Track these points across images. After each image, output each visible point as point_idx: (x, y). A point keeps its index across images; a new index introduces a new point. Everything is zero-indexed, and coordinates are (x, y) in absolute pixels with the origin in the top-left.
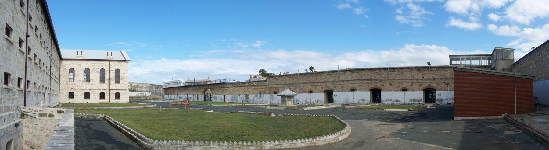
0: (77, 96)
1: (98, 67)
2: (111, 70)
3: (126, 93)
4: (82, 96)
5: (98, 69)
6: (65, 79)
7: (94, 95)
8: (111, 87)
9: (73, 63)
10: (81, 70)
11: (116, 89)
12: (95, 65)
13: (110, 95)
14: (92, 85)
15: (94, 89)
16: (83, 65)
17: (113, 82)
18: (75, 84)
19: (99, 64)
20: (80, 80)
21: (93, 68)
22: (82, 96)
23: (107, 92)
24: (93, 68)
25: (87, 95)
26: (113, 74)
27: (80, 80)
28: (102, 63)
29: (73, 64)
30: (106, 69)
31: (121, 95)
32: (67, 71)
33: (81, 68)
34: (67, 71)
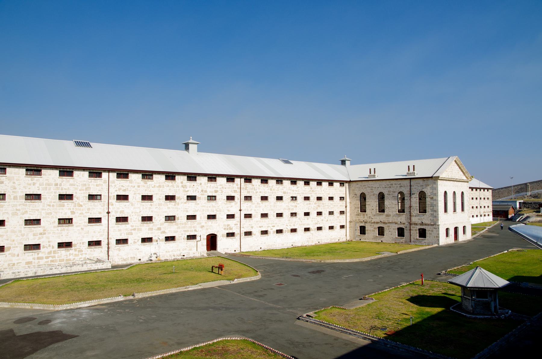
0: (369, 232)
1: (395, 190)
2: (413, 194)
3: (434, 229)
4: (374, 231)
5: (394, 192)
6: (356, 208)
7: (390, 231)
8: (414, 219)
9: (364, 186)
10: (374, 195)
11: (420, 222)
12: (390, 187)
13: (412, 231)
14: (387, 216)
15: (390, 222)
16: (376, 188)
17: (415, 211)
18: (367, 215)
19: (396, 186)
20: (373, 209)
21: (389, 191)
22: (374, 231)
23: (406, 227)
24: (389, 191)
25: (381, 231)
26: (415, 200)
27: (373, 209)
28: (400, 184)
29: (364, 187)
30: (406, 191)
31: (427, 232)
32: (357, 197)
33: (373, 192)
34: (357, 197)
